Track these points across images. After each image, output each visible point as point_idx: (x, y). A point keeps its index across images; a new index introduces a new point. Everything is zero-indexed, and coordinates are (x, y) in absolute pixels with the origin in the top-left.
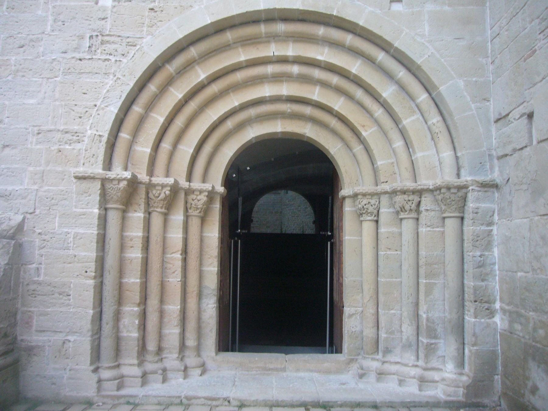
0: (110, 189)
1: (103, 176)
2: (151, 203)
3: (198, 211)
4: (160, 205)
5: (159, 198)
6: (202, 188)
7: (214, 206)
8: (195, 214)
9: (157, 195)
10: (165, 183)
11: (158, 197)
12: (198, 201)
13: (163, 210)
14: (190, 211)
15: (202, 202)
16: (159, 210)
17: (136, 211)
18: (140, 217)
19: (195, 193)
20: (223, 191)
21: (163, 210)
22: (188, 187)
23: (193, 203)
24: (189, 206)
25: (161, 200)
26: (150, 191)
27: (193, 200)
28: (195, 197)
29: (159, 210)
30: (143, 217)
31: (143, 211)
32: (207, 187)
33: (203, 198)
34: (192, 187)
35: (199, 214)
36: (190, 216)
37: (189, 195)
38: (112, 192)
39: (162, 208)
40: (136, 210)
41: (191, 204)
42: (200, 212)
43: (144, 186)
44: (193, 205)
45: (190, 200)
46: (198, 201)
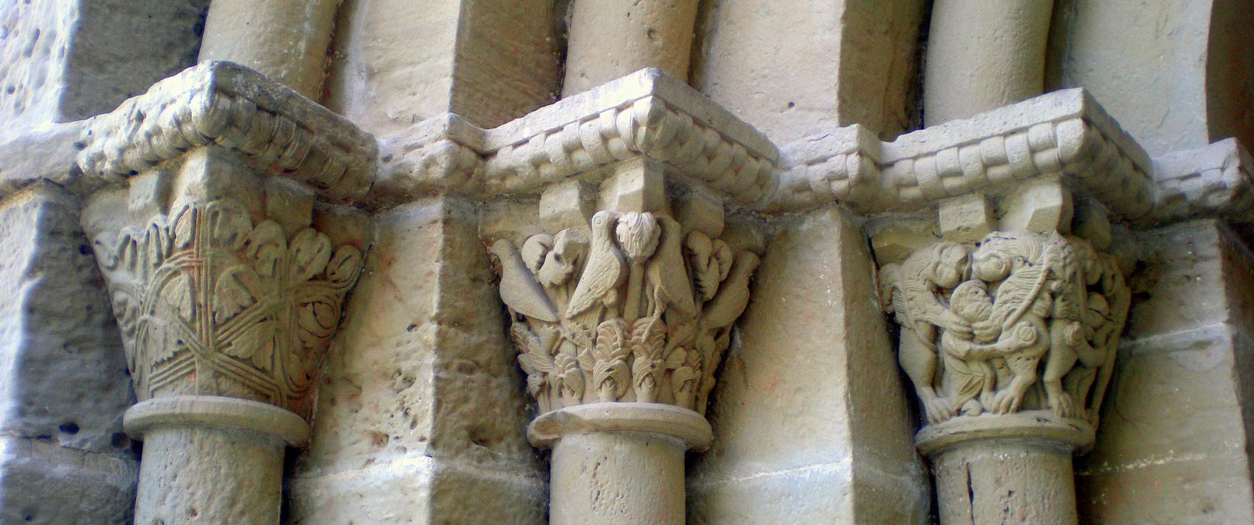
0: (119, 258)
1: (57, 164)
2: (534, 358)
3: (1012, 390)
4: (600, 369)
5: (580, 297)
6: (992, 148)
7: (1179, 335)
8: (990, 421)
9: (552, 271)
10: (589, 134)
11: (571, 280)
12: (990, 285)
13: (639, 405)
14: (932, 403)
15: (1022, 288)
16: (599, 407)
17: (380, 439)
18: (402, 485)
19: (952, 217)
20: (1231, 177)
21: (639, 405)
22: (853, 164)
23: (944, 316)
24: (916, 356)
25: (599, 309)
26: (500, 249)
27: (941, 292)
28: (945, 261)
29: (599, 407)
30: (425, 479)
31: (426, 427)
32: (1038, 134)
33: (1029, 246)
34: (902, 169)
35: (1027, 420)
36: (949, 447)
37: (901, 257)
38: (137, 281)
39: (619, 384)
40: (383, 428)
41: (936, 332)
42: (1032, 396)
43: (434, 209)
44: (948, 340)
45: (918, 307)
46: (990, 285)
